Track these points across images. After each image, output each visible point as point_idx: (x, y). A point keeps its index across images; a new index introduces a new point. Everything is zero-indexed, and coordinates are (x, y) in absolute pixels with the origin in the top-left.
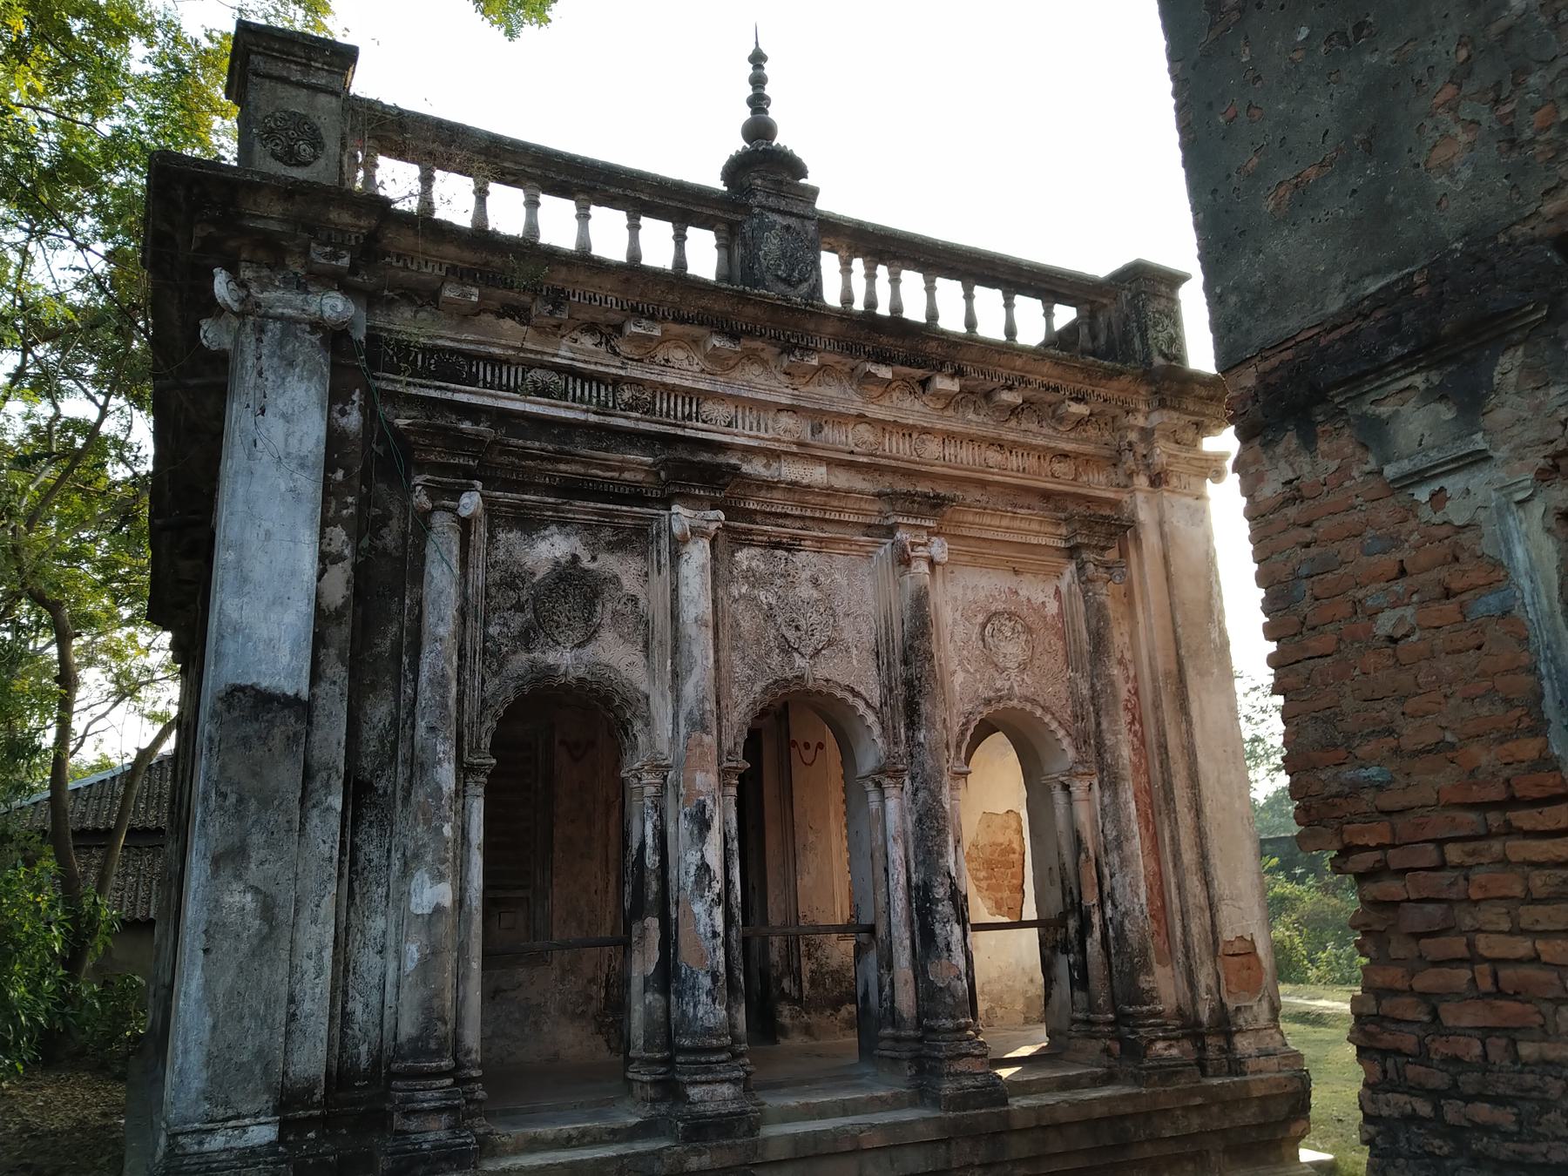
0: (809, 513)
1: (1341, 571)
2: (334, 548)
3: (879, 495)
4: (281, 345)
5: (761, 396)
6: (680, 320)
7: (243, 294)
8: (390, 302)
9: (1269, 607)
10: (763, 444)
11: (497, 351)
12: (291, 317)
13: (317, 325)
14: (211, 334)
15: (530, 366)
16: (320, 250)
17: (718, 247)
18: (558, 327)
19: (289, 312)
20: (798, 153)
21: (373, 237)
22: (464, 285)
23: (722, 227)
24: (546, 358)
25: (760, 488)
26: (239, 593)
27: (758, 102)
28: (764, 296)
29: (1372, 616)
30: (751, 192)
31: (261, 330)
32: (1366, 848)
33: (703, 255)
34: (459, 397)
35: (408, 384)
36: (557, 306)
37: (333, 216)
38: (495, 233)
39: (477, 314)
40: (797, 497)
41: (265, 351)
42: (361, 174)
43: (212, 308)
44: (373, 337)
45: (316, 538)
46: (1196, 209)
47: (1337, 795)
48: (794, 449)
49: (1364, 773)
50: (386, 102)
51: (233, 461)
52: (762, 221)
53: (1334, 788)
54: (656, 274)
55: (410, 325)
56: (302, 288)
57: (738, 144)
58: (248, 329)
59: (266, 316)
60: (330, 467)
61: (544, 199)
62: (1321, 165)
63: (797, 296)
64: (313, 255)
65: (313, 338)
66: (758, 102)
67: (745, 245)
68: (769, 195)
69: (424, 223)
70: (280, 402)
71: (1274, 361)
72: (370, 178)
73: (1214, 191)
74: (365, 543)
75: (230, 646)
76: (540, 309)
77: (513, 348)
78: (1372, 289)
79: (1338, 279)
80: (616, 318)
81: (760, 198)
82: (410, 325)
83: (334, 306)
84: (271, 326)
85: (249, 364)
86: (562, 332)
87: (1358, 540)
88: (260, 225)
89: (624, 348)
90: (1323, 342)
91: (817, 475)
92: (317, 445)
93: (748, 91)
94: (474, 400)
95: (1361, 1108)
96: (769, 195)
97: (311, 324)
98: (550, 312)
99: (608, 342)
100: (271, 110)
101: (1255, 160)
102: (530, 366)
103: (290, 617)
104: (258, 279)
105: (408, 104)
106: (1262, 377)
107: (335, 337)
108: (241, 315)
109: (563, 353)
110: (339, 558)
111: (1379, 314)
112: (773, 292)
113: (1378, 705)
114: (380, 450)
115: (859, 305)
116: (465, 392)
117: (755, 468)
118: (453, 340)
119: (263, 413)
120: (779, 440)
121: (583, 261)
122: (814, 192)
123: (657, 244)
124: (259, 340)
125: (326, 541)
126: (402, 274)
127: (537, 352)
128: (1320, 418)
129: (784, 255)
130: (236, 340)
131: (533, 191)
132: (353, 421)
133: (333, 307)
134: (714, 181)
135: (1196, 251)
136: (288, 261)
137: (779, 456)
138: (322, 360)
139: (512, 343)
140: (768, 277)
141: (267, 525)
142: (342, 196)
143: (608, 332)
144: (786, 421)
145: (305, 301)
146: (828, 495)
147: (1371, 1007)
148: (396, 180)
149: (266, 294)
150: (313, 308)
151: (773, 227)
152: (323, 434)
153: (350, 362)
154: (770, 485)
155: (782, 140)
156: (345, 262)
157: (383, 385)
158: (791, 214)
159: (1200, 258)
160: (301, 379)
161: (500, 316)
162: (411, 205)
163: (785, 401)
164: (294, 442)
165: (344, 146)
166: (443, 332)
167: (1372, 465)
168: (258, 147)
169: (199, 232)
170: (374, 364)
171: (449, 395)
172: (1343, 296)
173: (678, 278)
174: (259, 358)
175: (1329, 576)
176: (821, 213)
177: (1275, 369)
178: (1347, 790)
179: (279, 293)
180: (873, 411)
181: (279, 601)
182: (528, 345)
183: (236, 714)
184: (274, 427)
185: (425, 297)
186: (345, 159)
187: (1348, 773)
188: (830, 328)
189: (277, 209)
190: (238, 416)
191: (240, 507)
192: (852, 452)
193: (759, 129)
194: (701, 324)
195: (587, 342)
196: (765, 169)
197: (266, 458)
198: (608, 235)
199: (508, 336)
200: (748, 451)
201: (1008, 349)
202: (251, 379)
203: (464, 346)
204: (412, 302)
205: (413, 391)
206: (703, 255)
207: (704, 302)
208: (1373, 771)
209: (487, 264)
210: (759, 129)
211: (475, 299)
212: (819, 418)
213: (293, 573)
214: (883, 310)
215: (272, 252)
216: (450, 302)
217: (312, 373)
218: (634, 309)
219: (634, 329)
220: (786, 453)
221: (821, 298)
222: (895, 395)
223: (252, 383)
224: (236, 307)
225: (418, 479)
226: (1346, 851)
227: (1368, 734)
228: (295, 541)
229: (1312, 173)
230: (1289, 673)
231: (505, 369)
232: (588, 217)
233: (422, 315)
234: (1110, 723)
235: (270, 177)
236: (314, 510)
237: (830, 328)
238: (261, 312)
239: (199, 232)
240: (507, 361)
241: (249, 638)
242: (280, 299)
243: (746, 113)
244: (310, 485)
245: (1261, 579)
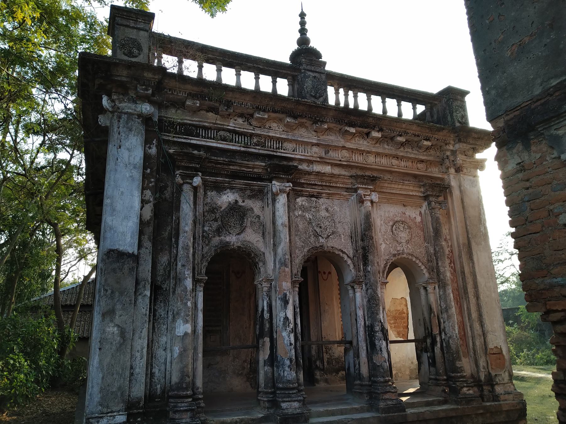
0: (324, 184)
1: (543, 198)
2: (147, 198)
3: (351, 176)
4: (127, 123)
5: (305, 140)
6: (275, 112)
7: (113, 104)
8: (167, 107)
9: (511, 214)
10: (306, 158)
11: (207, 124)
12: (131, 113)
13: (140, 116)
14: (102, 120)
15: (219, 130)
16: (141, 87)
17: (288, 85)
18: (229, 115)
19: (130, 111)
20: (318, 49)
21: (160, 82)
22: (194, 100)
23: (290, 77)
24: (225, 127)
25: (305, 174)
26: (112, 215)
27: (303, 31)
28: (306, 102)
29: (557, 216)
30: (301, 64)
31: (120, 117)
32: (557, 311)
33: (283, 87)
34: (192, 142)
35: (174, 137)
36: (229, 107)
37: (145, 74)
38: (205, 80)
39: (199, 111)
40: (320, 178)
41: (121, 125)
42: (156, 61)
43: (103, 111)
44: (160, 120)
45: (140, 194)
46: (477, 58)
47: (544, 289)
48: (318, 159)
49: (555, 280)
50: (165, 34)
51: (110, 165)
52: (305, 75)
53: (542, 286)
54: (265, 94)
55: (175, 115)
56: (135, 102)
57: (295, 47)
58: (115, 118)
59: (121, 112)
60: (145, 168)
61: (224, 68)
62: (531, 36)
63: (319, 102)
64: (138, 89)
65: (139, 121)
66: (303, 31)
67: (299, 84)
68: (307, 65)
69: (180, 77)
70: (127, 144)
71: (512, 116)
72: (160, 61)
73: (485, 50)
74: (158, 195)
75: (108, 235)
76: (222, 108)
77: (213, 123)
78: (554, 84)
79: (539, 81)
80: (251, 111)
81: (304, 66)
82: (175, 115)
83: (146, 108)
84: (123, 116)
85: (115, 130)
86: (231, 117)
87: (550, 186)
88: (119, 79)
89: (254, 123)
90: (533, 107)
91: (327, 169)
92: (140, 160)
93: (299, 27)
94: (198, 143)
95: (558, 418)
96: (307, 65)
97: (138, 115)
98: (226, 109)
99: (248, 121)
100: (123, 37)
101: (502, 36)
102: (219, 130)
103: (130, 224)
104: (118, 99)
105: (173, 35)
106: (506, 122)
107: (147, 120)
108: (112, 112)
109: (231, 125)
110: (148, 202)
111: (557, 94)
112: (309, 100)
113: (560, 252)
114: (163, 161)
115: (342, 105)
116: (195, 140)
117: (304, 167)
118: (190, 120)
119: (120, 148)
120: (312, 156)
121: (238, 90)
122: (324, 64)
123: (265, 83)
124: (119, 121)
125: (144, 195)
126: (171, 96)
127: (222, 125)
128: (532, 137)
129: (313, 87)
130: (111, 122)
131: (220, 66)
132: (153, 151)
133: (146, 109)
134: (286, 60)
135: (477, 74)
136: (130, 92)
137: (312, 163)
138: (142, 128)
139: (212, 121)
140: (308, 95)
141: (121, 190)
142: (149, 67)
143: (248, 117)
144: (315, 149)
145: (136, 107)
146: (331, 177)
147: (561, 377)
148: (169, 62)
149: (121, 104)
150: (139, 109)
151: (309, 77)
152: (142, 156)
153: (152, 129)
154: (309, 173)
155: (312, 44)
156: (150, 92)
157: (165, 137)
158: (316, 72)
159: (479, 77)
160: (134, 136)
161: (207, 111)
162: (175, 71)
163: (315, 141)
164: (131, 159)
165: (150, 50)
166: (187, 118)
167: (556, 154)
168: (118, 51)
169: (97, 82)
170: (161, 130)
171: (189, 141)
172: (541, 87)
173: (274, 95)
174: (118, 128)
175: (538, 201)
176: (327, 71)
177: (512, 119)
178: (548, 287)
179: (126, 104)
180: (348, 145)
181: (126, 218)
182: (218, 122)
183: (111, 260)
184: (124, 153)
185: (179, 105)
186: (150, 55)
187: (548, 281)
188: (331, 113)
189: (125, 73)
190: (112, 149)
191: (112, 183)
192: (340, 161)
193: (303, 41)
194: (283, 113)
195: (240, 121)
196: (306, 56)
197: (121, 165)
198: (248, 80)
199: (210, 119)
200: (301, 161)
201: (399, 120)
202: (116, 135)
203: (194, 123)
204: (175, 107)
205: (175, 139)
206: (283, 87)
207: (284, 104)
208: (559, 279)
209: (202, 92)
210: (303, 41)
211: (198, 105)
212: (328, 148)
213: (132, 207)
214: (351, 106)
215: (123, 89)
216: (189, 106)
217: (138, 133)
218: (257, 108)
219: (258, 115)
221: (328, 103)
222: (356, 139)
223: (116, 137)
224: (110, 109)
225: (178, 172)
226: (548, 312)
227: (556, 264)
228: (132, 195)
229: (527, 39)
230: (522, 240)
231: (209, 131)
232: (240, 75)
233: (179, 111)
235: (123, 60)
236: (139, 184)
237: (331, 113)
238: (120, 111)
239: (97, 82)
240: (210, 128)
241: (115, 231)
242: (127, 106)
243: (298, 35)
244: (138, 175)
245: (508, 203)
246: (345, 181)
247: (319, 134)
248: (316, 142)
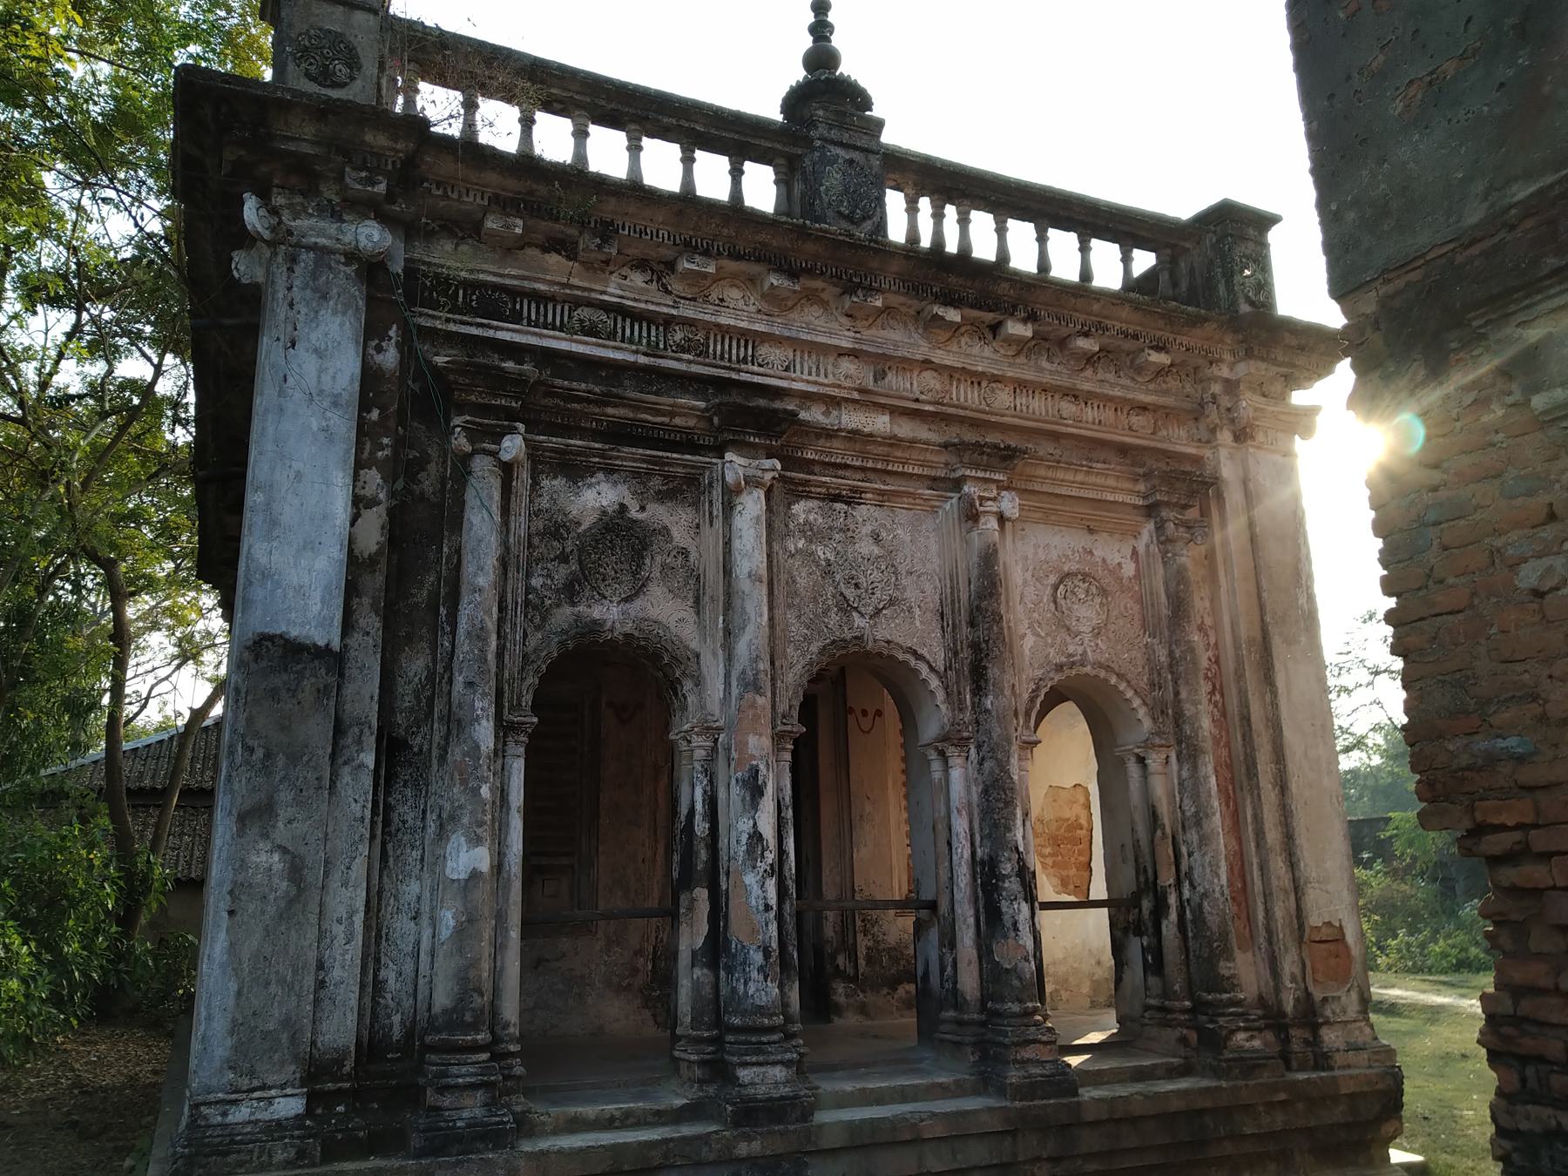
0: (870, 464)
1: (1477, 516)
2: (368, 492)
3: (946, 446)
4: (314, 275)
6: (736, 256)
7: (274, 221)
8: (429, 235)
9: (1386, 559)
10: (822, 390)
11: (542, 287)
12: (324, 247)
13: (352, 256)
14: (244, 266)
15: (577, 303)
16: (354, 174)
17: (776, 182)
18: (607, 262)
19: (322, 241)
20: (863, 83)
21: (410, 162)
22: (508, 215)
23: (782, 161)
24: (594, 295)
25: (818, 436)
26: (268, 537)
27: (821, 30)
28: (826, 231)
29: (1514, 566)
30: (812, 124)
31: (293, 260)
32: (1503, 828)
33: (761, 188)
34: (501, 335)
35: (448, 320)
36: (606, 239)
37: (369, 138)
38: (540, 159)
39: (522, 248)
40: (858, 447)
41: (297, 283)
42: (400, 100)
43: (245, 239)
44: (411, 270)
45: (349, 480)
46: (1309, 117)
47: (1469, 768)
48: (856, 395)
49: (1501, 743)
50: (428, 23)
51: (263, 400)
52: (823, 155)
53: (1465, 760)
54: (710, 206)
55: (451, 259)
56: (337, 216)
57: (798, 74)
58: (280, 259)
59: (299, 245)
60: (364, 405)
61: (593, 129)
62: (1462, 58)
63: (861, 233)
64: (348, 180)
65: (348, 270)
66: (821, 30)
67: (805, 180)
68: (831, 127)
69: (469, 149)
70: (313, 337)
71: (1400, 283)
72: (410, 102)
73: (1332, 96)
74: (400, 484)
75: (258, 593)
76: (587, 242)
77: (559, 284)
78: (1521, 196)
79: (1479, 187)
80: (668, 253)
81: (822, 130)
82: (451, 259)
83: (370, 235)
84: (304, 256)
85: (280, 295)
86: (611, 268)
87: (1496, 482)
88: (292, 147)
89: (677, 286)
90: (1459, 259)
91: (881, 423)
92: (352, 381)
93: (810, 18)
94: (518, 338)
95: (1494, 1118)
96: (831, 127)
97: (345, 254)
98: (599, 246)
99: (659, 279)
100: (305, 27)
101: (1381, 58)
102: (577, 303)
103: (321, 563)
104: (290, 206)
105: (449, 26)
106: (1383, 303)
107: (371, 269)
108: (272, 244)
109: (612, 290)
110: (372, 503)
111: (1529, 223)
112: (834, 227)
113: (1519, 667)
114: (416, 387)
115: (926, 242)
116: (508, 330)
117: (814, 415)
118: (495, 274)
119: (293, 346)
120: (839, 386)
121: (634, 190)
122: (879, 124)
123: (712, 176)
124: (291, 270)
125: (360, 484)
126: (442, 204)
127: (584, 289)
128: (1454, 345)
129: (846, 190)
130: (268, 273)
131: (582, 120)
132: (389, 358)
133: (369, 237)
134: (773, 111)
135: (1307, 164)
136: (323, 188)
138: (357, 293)
139: (558, 279)
140: (830, 213)
141: (296, 466)
142: (379, 117)
143: (659, 270)
144: (847, 366)
145: (340, 230)
146: (891, 445)
147: (1507, 1006)
148: (438, 105)
149: (298, 222)
150: (348, 238)
151: (835, 161)
152: (358, 371)
153: (387, 296)
154: (829, 434)
155: (846, 69)
156: (381, 188)
157: (423, 321)
158: (855, 148)
159: (1313, 171)
160: (335, 313)
161: (546, 250)
162: (455, 130)
163: (845, 344)
164: (326, 378)
165: (382, 67)
166: (485, 267)
167: (1517, 396)
168: (291, 67)
169: (229, 155)
170: (411, 299)
171: (490, 333)
172: (1485, 205)
173: (735, 210)
174: (290, 289)
175: (1462, 522)
176: (886, 147)
177: (1398, 293)
178: (1480, 762)
179: (313, 221)
180: (939, 357)
181: (310, 546)
182: (575, 281)
183: (264, 664)
184: (305, 364)
185: (466, 229)
186: (384, 82)
187: (1482, 744)
188: (895, 266)
189: (309, 130)
190: (269, 350)
191: (269, 446)
192: (917, 400)
193: (821, 58)
194: (758, 260)
195: (638, 279)
196: (827, 99)
197: (298, 395)
198: (661, 164)
199: (553, 272)
200: (806, 397)
201: (1083, 289)
202: (282, 312)
203: (507, 282)
204: (452, 234)
205: (452, 327)
206: (761, 188)
207: (763, 237)
208: (1512, 741)
209: (531, 193)
210: (821, 58)
211: (518, 231)
212: (883, 363)
213: (325, 517)
214: (952, 247)
215: (304, 178)
216: (493, 234)
217: (347, 306)
218: (687, 244)
219: (687, 265)
220: (847, 400)
221: (885, 235)
223: (282, 317)
224: (267, 235)
225: (457, 421)
226: (1479, 831)
227: (1506, 700)
228: (327, 483)
229: (1450, 68)
231: (550, 307)
232: (640, 148)
233: (464, 248)
234: (1211, 678)
235: (303, 94)
236: (347, 451)
237: (895, 266)
238: (294, 240)
239: (229, 155)
240: (552, 299)
241: (278, 584)
242: (313, 228)
243: (807, 42)
244: (344, 425)
245: (1379, 528)
246: (929, 457)
247: (859, 324)
248: (850, 345)
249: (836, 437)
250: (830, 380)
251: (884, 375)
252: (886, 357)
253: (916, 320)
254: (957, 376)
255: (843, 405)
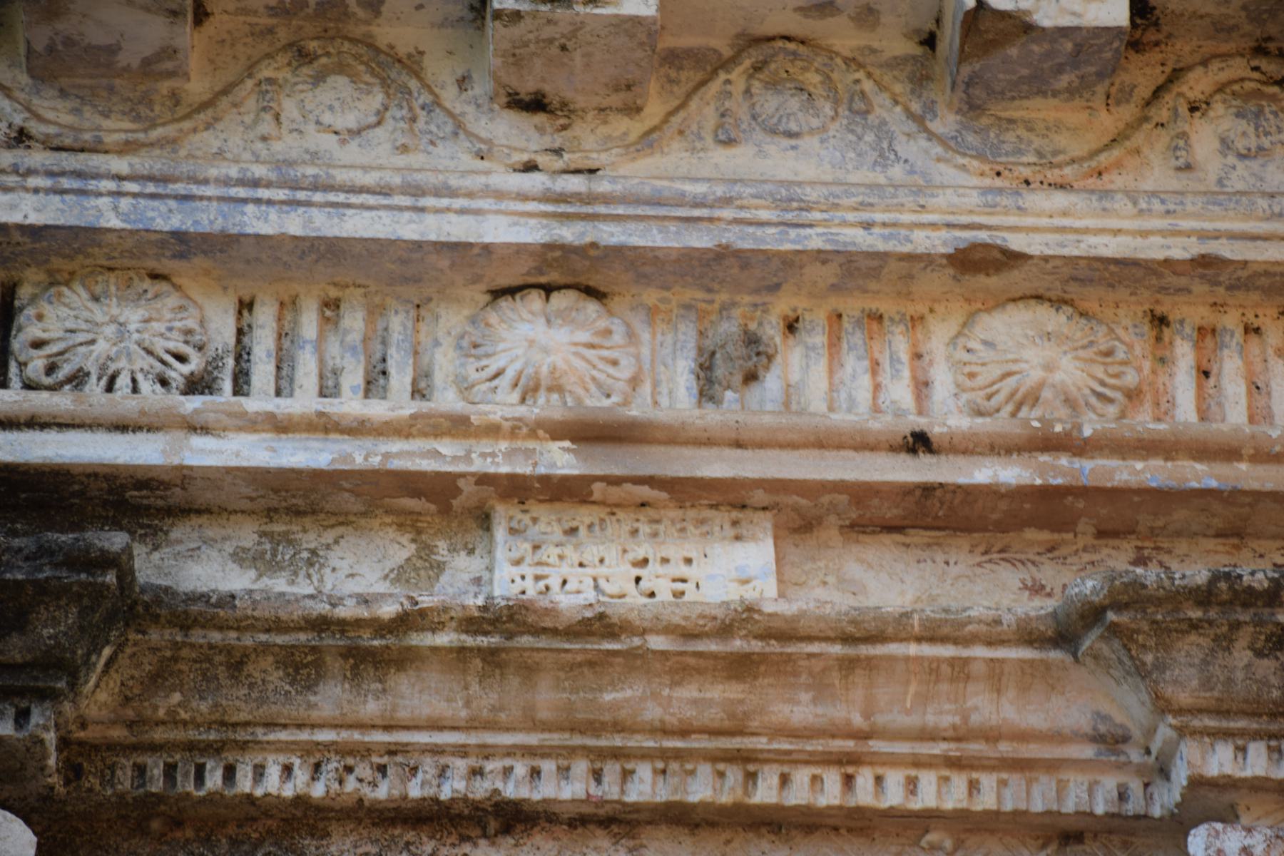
0: (645, 787)
3: (1064, 633)
5: (359, 225)
10: (361, 455)
25: (303, 668)
40: (547, 697)
48: (560, 460)
91: (734, 570)
117: (206, 568)
120: (458, 426)
137: (484, 521)
144: (543, 342)
146: (740, 667)
154: (371, 649)
163: (499, 229)
180: (1051, 223)
192: (919, 443)
200: (293, 505)
212: (739, 296)
220: (518, 490)
222: (1204, 138)
246: (986, 708)
247: (589, 139)
248: (531, 233)
249: (404, 660)
250: (396, 404)
251: (754, 361)
252: (763, 272)
253: (921, 80)
254: (1191, 313)
255: (503, 514)
